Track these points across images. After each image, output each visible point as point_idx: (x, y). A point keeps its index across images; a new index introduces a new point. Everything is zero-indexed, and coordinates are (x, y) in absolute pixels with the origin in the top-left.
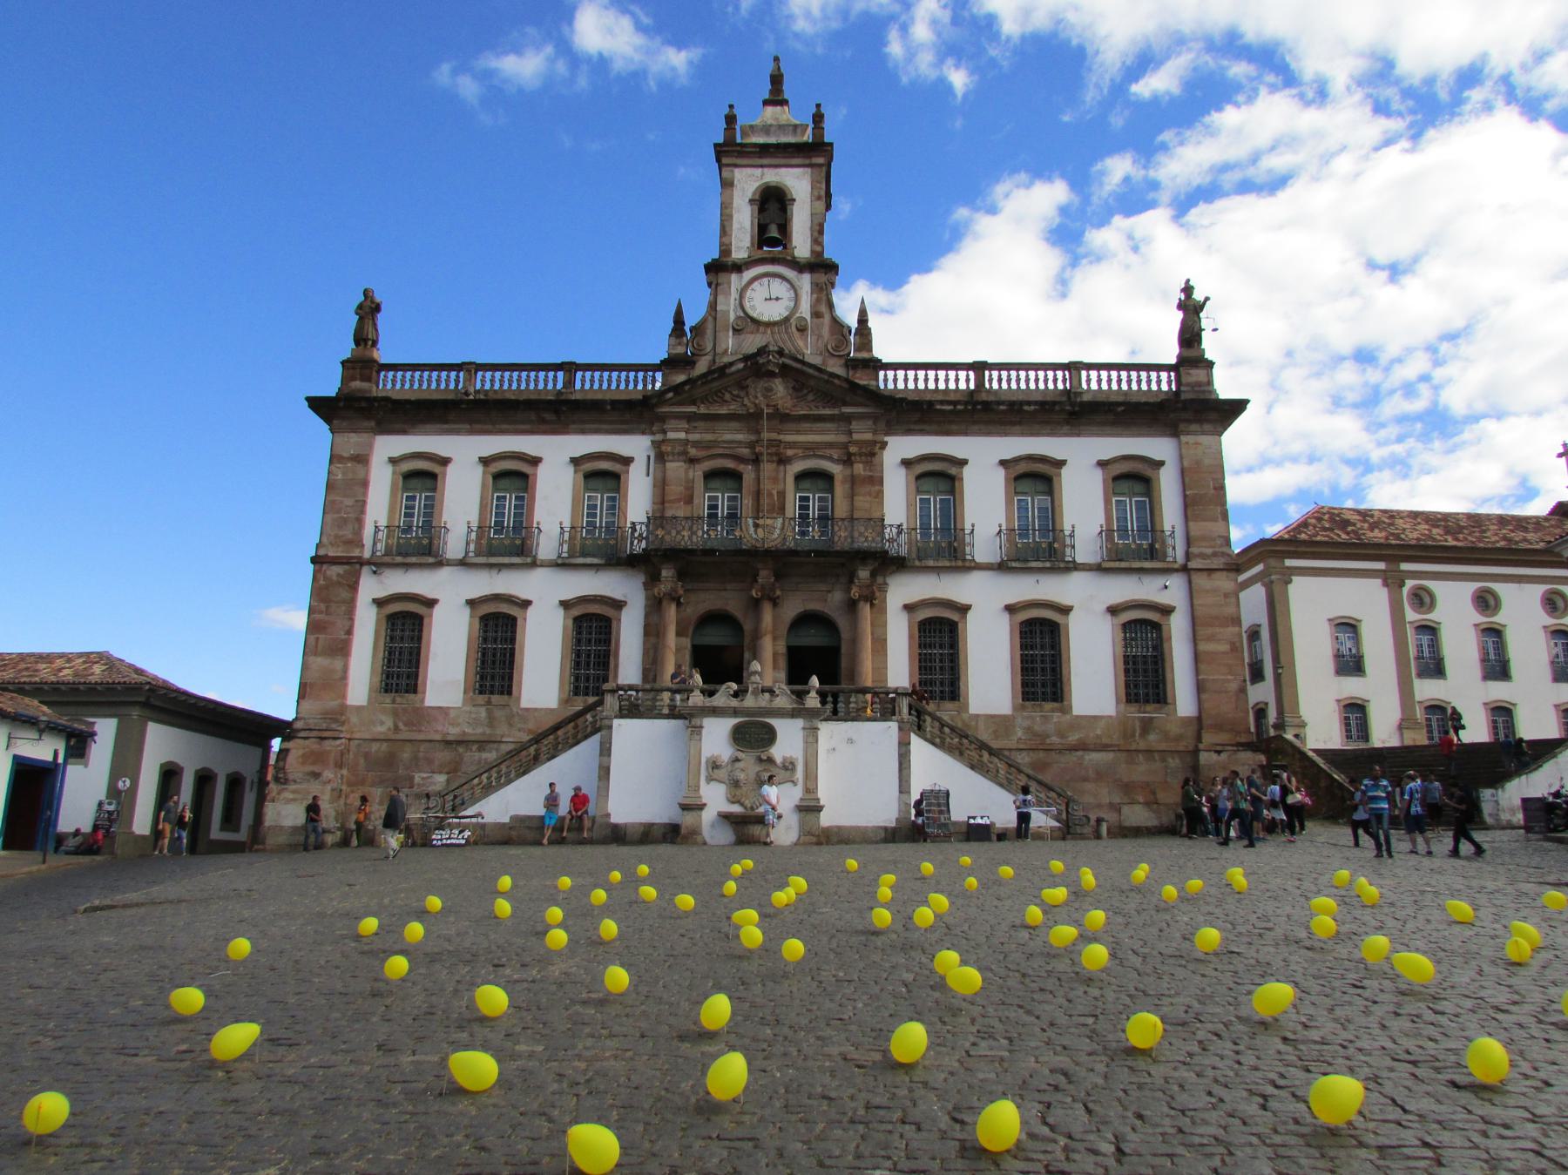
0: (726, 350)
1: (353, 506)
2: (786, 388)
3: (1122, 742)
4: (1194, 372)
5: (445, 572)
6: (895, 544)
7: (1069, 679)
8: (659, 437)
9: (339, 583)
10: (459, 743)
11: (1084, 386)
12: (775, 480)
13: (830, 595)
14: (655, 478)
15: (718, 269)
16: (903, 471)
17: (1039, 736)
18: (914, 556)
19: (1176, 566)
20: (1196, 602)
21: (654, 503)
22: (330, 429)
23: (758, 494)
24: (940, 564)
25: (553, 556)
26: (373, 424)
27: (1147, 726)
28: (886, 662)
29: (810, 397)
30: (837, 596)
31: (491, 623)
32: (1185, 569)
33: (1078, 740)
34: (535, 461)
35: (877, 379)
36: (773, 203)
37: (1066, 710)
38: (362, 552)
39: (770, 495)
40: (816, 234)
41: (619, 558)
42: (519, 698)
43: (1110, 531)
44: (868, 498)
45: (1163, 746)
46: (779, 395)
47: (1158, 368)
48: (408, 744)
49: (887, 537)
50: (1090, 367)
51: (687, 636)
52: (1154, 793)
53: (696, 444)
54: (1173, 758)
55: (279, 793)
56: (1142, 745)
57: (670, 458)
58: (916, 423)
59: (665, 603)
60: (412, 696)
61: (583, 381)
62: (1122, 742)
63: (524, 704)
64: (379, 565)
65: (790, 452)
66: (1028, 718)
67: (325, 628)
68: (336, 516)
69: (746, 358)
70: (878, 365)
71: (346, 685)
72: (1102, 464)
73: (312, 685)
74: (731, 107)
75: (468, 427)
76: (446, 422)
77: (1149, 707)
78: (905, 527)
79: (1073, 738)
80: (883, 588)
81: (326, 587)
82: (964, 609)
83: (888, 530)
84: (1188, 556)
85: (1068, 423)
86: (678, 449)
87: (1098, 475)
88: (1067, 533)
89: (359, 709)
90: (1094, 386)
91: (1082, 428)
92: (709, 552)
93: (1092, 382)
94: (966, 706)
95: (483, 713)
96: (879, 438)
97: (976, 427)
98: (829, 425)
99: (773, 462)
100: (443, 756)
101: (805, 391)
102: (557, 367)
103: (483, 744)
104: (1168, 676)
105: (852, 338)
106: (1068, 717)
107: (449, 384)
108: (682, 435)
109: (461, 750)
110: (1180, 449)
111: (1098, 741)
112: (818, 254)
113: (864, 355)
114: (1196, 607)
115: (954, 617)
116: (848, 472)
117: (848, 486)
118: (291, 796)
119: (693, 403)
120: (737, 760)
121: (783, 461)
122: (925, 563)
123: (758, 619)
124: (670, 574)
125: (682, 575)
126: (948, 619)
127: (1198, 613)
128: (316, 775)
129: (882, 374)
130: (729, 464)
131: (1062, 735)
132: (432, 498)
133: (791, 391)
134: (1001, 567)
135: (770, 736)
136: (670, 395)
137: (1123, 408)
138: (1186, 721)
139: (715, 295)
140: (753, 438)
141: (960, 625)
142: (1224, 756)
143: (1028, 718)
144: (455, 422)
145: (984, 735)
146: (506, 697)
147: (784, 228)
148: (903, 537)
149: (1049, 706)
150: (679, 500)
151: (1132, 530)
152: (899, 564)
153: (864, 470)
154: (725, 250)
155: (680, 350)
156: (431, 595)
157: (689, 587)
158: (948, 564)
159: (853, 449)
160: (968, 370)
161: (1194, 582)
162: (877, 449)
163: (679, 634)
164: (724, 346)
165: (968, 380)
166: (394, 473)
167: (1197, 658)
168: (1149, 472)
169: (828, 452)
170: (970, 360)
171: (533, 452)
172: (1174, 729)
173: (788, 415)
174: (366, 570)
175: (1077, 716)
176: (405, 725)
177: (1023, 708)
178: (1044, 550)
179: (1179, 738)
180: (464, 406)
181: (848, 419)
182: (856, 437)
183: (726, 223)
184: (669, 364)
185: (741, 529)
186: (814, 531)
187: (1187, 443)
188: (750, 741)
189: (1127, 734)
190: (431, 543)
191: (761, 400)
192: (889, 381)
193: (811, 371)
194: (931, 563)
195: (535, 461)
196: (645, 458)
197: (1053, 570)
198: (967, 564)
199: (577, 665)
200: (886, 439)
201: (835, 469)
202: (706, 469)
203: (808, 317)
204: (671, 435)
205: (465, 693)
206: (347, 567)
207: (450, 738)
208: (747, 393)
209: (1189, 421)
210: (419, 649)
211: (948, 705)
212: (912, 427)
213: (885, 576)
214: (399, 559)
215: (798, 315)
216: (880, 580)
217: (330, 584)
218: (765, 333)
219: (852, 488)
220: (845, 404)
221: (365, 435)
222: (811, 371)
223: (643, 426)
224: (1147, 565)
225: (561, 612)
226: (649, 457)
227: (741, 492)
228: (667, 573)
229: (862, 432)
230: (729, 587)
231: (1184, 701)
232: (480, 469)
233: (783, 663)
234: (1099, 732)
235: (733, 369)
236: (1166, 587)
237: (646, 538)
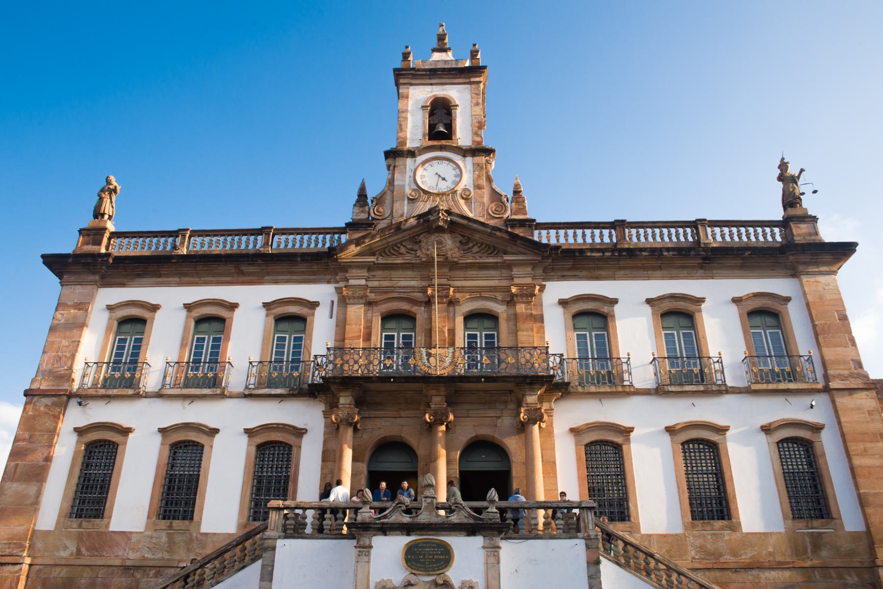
1: (69, 346)
3: (795, 559)
6: (559, 371)
13: (499, 421)
14: (337, 319)
16: (560, 310)
17: (713, 554)
22: (60, 283)
23: (429, 332)
24: (602, 390)
25: (241, 389)
26: (97, 277)
29: (476, 249)
30: (507, 421)
32: (826, 390)
33: (751, 558)
35: (533, 235)
37: (735, 527)
38: (71, 386)
39: (442, 332)
41: (301, 389)
46: (448, 247)
47: (771, 224)
48: (88, 569)
49: (551, 365)
51: (363, 462)
53: (374, 290)
58: (570, 269)
59: (342, 428)
60: (97, 521)
64: (83, 398)
66: (700, 536)
67: (26, 455)
69: (419, 217)
75: (177, 279)
76: (160, 276)
79: (746, 556)
81: (34, 417)
82: (627, 432)
83: (552, 359)
84: (826, 377)
85: (702, 267)
89: (47, 533)
90: (719, 239)
91: (714, 271)
92: (384, 379)
94: (636, 528)
97: (622, 272)
99: (443, 303)
101: (471, 245)
104: (829, 491)
106: (738, 534)
108: (363, 282)
109: (138, 576)
111: (772, 558)
114: (843, 424)
115: (618, 440)
116: (511, 311)
117: (511, 323)
120: (410, 584)
121: (452, 303)
122: (586, 390)
124: (348, 402)
130: (405, 306)
131: (735, 553)
132: (140, 340)
133: (458, 244)
134: (659, 391)
135: (445, 557)
137: (750, 253)
140: (424, 283)
141: (624, 447)
144: (167, 276)
146: (187, 522)
147: (450, 127)
149: (718, 524)
153: (526, 309)
155: (364, 216)
157: (366, 414)
158: (609, 390)
164: (400, 212)
165: (610, 236)
166: (110, 319)
168: (776, 306)
173: (457, 263)
174: (73, 402)
175: (747, 534)
176: (88, 550)
177: (693, 526)
178: (696, 375)
180: (174, 261)
185: (415, 358)
188: (423, 563)
189: (798, 550)
190: (133, 377)
192: (542, 237)
193: (475, 226)
194: (593, 389)
196: (329, 303)
197: (706, 393)
201: (499, 309)
203: (472, 190)
204: (352, 282)
206: (55, 399)
207: (128, 563)
208: (420, 246)
209: (807, 264)
212: (565, 273)
220: (506, 253)
221: (89, 287)
222: (475, 226)
223: (329, 277)
224: (792, 386)
226: (333, 302)
227: (415, 332)
228: (345, 400)
229: (522, 277)
230: (403, 414)
232: (184, 313)
234: (771, 549)
236: (812, 407)
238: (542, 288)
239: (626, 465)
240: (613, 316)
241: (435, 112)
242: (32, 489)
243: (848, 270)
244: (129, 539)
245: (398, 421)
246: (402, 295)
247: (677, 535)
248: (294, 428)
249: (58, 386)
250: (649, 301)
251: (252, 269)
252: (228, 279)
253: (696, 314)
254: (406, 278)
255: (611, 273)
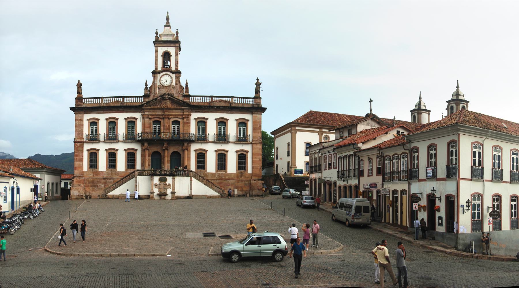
0: (157, 93)
2: (170, 102)
4: (257, 100)
5: (101, 143)
7: (227, 166)
8: (143, 113)
9: (80, 147)
10: (106, 178)
11: (234, 102)
12: (168, 123)
13: (179, 148)
15: (155, 73)
16: (194, 121)
18: (196, 139)
19: (250, 143)
20: (253, 150)
21: (142, 128)
27: (242, 175)
28: (190, 162)
29: (175, 104)
31: (110, 154)
32: (251, 143)
34: (117, 119)
35: (189, 100)
36: (167, 56)
40: (176, 64)
42: (117, 170)
43: (237, 135)
44: (187, 127)
45: (244, 179)
46: (168, 104)
47: (250, 98)
50: (235, 97)
52: (242, 188)
53: (151, 115)
54: (246, 182)
55: (73, 189)
56: (241, 179)
57: (146, 118)
59: (146, 150)
61: (126, 100)
62: (236, 178)
63: (118, 171)
65: (171, 117)
67: (78, 156)
68: (78, 132)
70: (189, 96)
71: (83, 167)
72: (236, 120)
73: (77, 167)
74: (157, 30)
75: (103, 112)
77: (243, 171)
78: (195, 133)
79: (227, 178)
80: (190, 146)
81: (77, 147)
82: (206, 151)
84: (253, 141)
85: (230, 111)
86: (147, 116)
87: (235, 122)
88: (228, 135)
93: (236, 101)
95: (110, 173)
96: (189, 113)
98: (179, 110)
100: (103, 181)
102: (120, 97)
103: (110, 179)
104: (247, 165)
105: (184, 89)
107: (99, 101)
108: (148, 113)
110: (253, 117)
112: (177, 69)
113: (187, 94)
115: (204, 152)
116: (183, 121)
117: (183, 124)
118: (75, 189)
119: (150, 106)
121: (169, 119)
123: (164, 153)
125: (149, 144)
126: (203, 153)
127: (253, 153)
128: (79, 185)
129: (191, 98)
130: (158, 119)
133: (171, 102)
134: (214, 142)
136: (145, 105)
138: (250, 174)
139: (154, 79)
140: (163, 113)
142: (256, 181)
143: (218, 173)
145: (210, 178)
148: (194, 136)
150: (148, 128)
151: (242, 135)
152: (193, 142)
154: (156, 68)
155: (147, 93)
156: (98, 149)
157: (150, 146)
159: (184, 116)
160: (209, 97)
161: (253, 146)
162: (189, 116)
163: (148, 156)
164: (156, 92)
165: (209, 100)
167: (253, 162)
169: (179, 117)
170: (210, 95)
171: (117, 117)
172: (247, 176)
177: (218, 171)
179: (248, 178)
181: (183, 109)
182: (185, 113)
183: (156, 62)
184: (145, 96)
186: (176, 135)
187: (254, 116)
189: (238, 177)
191: (164, 105)
192: (192, 100)
195: (117, 119)
196: (140, 118)
198: (207, 142)
199: (128, 162)
200: (191, 113)
201: (180, 120)
202: (153, 120)
203: (175, 85)
204: (146, 113)
205: (106, 168)
207: (104, 177)
210: (97, 159)
211: (203, 170)
213: (190, 144)
214: (91, 141)
215: (172, 84)
216: (189, 145)
217: (78, 147)
218: (165, 89)
219: (184, 124)
220: (182, 106)
225: (124, 152)
229: (186, 113)
231: (250, 170)
232: (106, 121)
233: (169, 162)
234: (232, 176)
235: (158, 99)
237: (141, 137)
238: (190, 115)
239: (205, 158)
240: (207, 123)
241: (165, 57)
242: (81, 163)
243: (264, 115)
244: (103, 173)
245: (157, 148)
246: (157, 117)
247: (214, 173)
248: (135, 149)
249: (81, 140)
250: (216, 119)
251: (121, 109)
252: (115, 111)
253: (227, 123)
254: (158, 112)
255: (208, 111)
